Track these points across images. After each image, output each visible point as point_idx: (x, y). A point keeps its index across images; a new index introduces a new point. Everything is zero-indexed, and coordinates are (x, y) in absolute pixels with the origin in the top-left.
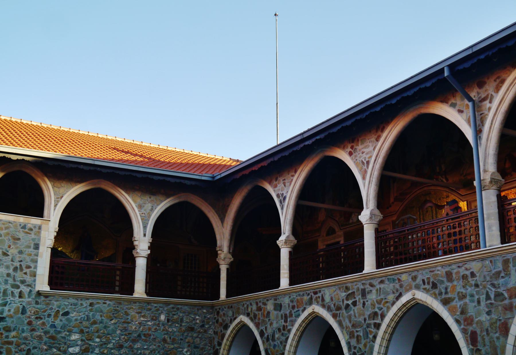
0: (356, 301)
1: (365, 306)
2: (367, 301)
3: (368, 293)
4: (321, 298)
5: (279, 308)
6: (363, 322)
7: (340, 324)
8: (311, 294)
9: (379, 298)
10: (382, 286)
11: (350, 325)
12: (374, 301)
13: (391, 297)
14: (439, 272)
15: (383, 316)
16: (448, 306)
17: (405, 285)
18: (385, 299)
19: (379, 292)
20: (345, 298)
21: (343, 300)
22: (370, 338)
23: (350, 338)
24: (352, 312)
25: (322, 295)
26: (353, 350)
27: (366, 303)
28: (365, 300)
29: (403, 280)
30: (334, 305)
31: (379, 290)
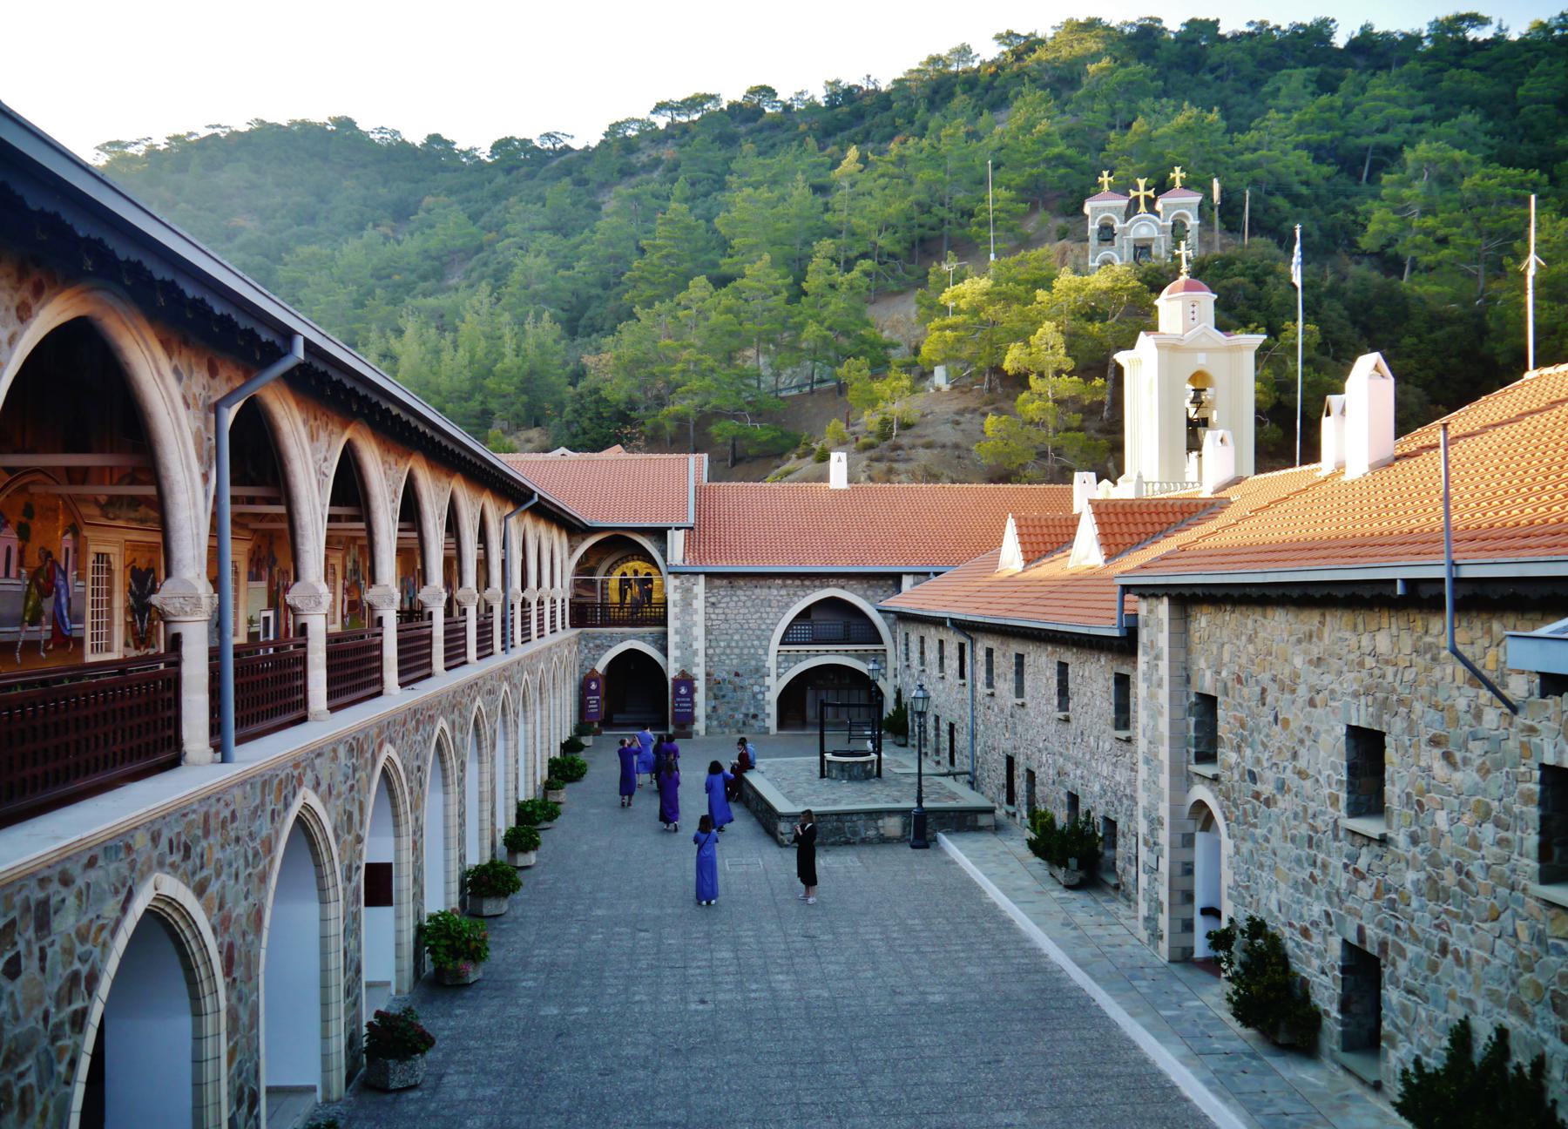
0: (18, 954)
1: (48, 964)
2: (52, 943)
3: (55, 913)
6: (40, 1026)
9: (85, 920)
10: (93, 875)
12: (69, 935)
13: (110, 908)
14: (194, 816)
15: (93, 979)
16: (203, 900)
17: (141, 859)
18: (98, 917)
19: (84, 899)
22: (59, 1073)
27: (50, 952)
28: (45, 943)
31: (85, 892)
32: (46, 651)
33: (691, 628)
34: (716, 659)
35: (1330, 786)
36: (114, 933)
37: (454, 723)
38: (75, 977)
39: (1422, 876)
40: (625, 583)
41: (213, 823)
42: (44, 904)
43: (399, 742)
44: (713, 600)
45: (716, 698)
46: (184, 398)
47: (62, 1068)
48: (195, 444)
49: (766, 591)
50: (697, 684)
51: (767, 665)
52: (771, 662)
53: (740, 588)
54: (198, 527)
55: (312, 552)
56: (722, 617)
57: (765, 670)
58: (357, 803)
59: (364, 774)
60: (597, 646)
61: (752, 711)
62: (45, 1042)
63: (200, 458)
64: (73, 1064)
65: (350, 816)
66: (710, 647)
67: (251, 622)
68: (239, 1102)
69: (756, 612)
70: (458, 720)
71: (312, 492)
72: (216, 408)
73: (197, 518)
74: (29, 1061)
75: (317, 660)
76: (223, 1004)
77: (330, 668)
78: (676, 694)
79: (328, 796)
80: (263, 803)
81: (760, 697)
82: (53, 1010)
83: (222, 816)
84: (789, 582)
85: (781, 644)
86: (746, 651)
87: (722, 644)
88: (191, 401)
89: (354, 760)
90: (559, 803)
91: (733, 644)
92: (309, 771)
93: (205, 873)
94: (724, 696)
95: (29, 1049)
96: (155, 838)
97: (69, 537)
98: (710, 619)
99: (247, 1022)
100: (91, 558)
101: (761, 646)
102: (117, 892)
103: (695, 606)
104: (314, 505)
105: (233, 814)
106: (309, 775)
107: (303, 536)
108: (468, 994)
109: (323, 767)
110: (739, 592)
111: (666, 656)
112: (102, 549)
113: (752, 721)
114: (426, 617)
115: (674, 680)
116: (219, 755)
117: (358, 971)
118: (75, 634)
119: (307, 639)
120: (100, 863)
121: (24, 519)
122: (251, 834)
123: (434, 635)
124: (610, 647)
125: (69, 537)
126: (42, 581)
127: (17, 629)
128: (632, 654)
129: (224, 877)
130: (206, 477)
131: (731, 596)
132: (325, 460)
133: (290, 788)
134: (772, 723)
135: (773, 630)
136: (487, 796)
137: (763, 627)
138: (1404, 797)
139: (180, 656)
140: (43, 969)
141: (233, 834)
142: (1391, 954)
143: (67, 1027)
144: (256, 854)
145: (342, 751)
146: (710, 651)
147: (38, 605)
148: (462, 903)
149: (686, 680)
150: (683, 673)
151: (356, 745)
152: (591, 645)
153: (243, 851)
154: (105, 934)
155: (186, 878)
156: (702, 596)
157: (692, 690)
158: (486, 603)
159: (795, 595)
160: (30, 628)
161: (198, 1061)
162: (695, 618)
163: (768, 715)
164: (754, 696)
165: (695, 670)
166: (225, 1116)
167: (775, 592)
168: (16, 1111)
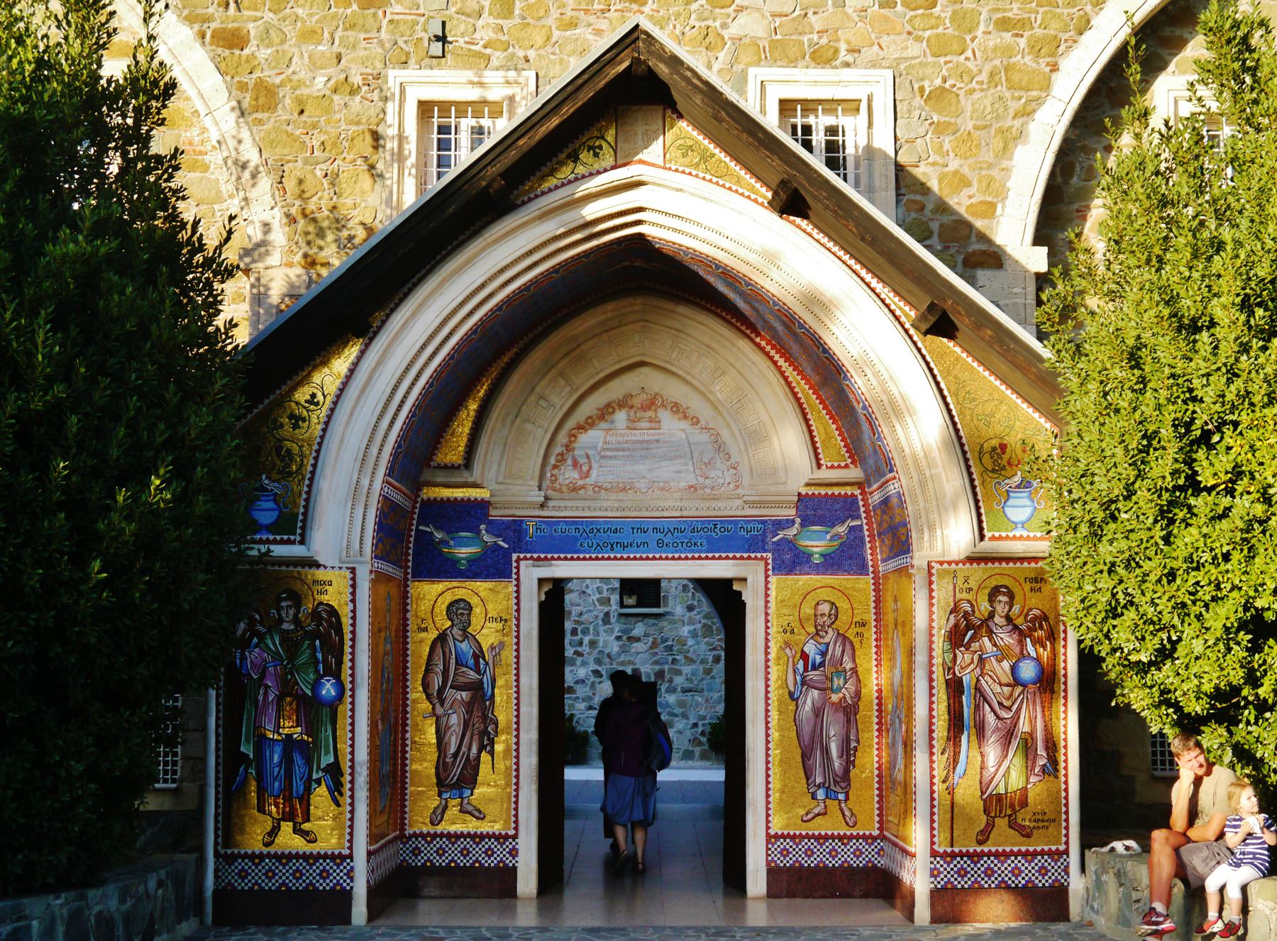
35: (600, 593)
39: (699, 626)
138: (680, 588)
142: (667, 676)
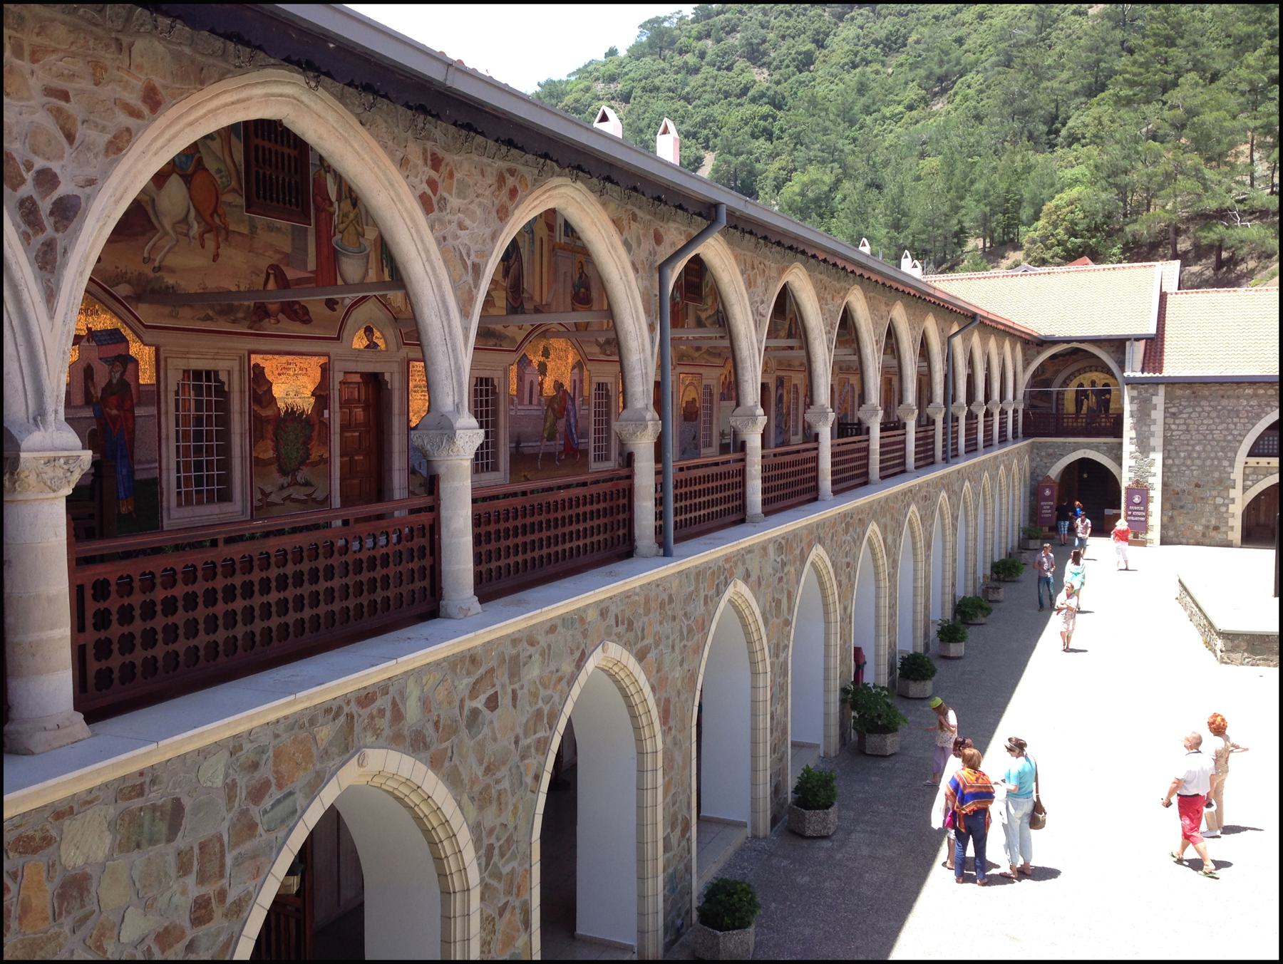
2: (522, 687)
3: (524, 665)
4: (388, 714)
5: (162, 827)
7: (453, 780)
8: (346, 710)
10: (552, 638)
11: (479, 771)
13: (567, 668)
14: (637, 598)
15: (553, 717)
18: (557, 671)
20: (467, 693)
21: (462, 701)
22: (526, 783)
23: (481, 808)
24: (486, 730)
25: (394, 704)
26: (486, 842)
27: (519, 693)
28: (516, 686)
29: (589, 619)
30: (436, 724)
32: (559, 460)
33: (1148, 438)
34: (1175, 469)
36: (571, 682)
37: (885, 526)
38: (539, 714)
40: (1081, 395)
41: (653, 605)
42: (515, 659)
43: (828, 541)
44: (1173, 410)
45: (1173, 508)
46: (633, 265)
47: (529, 780)
48: (643, 301)
49: (1233, 402)
50: (1152, 493)
51: (1232, 476)
52: (1237, 474)
53: (1205, 398)
54: (646, 368)
55: (750, 381)
56: (1184, 427)
57: (1229, 483)
58: (785, 592)
59: (792, 570)
60: (1050, 455)
61: (1213, 522)
62: (517, 758)
63: (647, 312)
64: (537, 778)
65: (778, 603)
66: (1169, 457)
67: (722, 435)
68: (673, 827)
69: (1222, 423)
70: (889, 522)
71: (751, 332)
72: (662, 269)
73: (645, 360)
74: (503, 772)
75: (754, 472)
76: (660, 746)
77: (764, 480)
78: (1130, 502)
79: (757, 587)
80: (697, 589)
81: (1223, 509)
82: (521, 736)
83: (660, 600)
84: (1261, 392)
85: (1251, 454)
86: (1208, 463)
87: (1182, 455)
88: (639, 266)
89: (783, 557)
90: (997, 601)
91: (1195, 455)
92: (740, 564)
93: (646, 642)
94: (1182, 507)
95: (504, 763)
96: (603, 614)
97: (576, 371)
98: (1170, 429)
99: (681, 764)
100: (594, 386)
101: (1226, 458)
102: (572, 653)
103: (1153, 417)
104: (752, 342)
105: (670, 597)
106: (740, 570)
107: (743, 368)
108: (884, 764)
109: (754, 565)
110: (1204, 403)
111: (1120, 465)
112: (601, 380)
113: (1213, 534)
114: (864, 431)
115: (1127, 489)
116: (661, 551)
117: (784, 732)
118: (581, 447)
119: (745, 455)
120: (560, 629)
121: (542, 359)
122: (685, 614)
123: (871, 447)
124: (1063, 456)
125: (576, 371)
126: (556, 406)
127: (538, 444)
128: (1085, 463)
129: (662, 647)
130: (651, 328)
131: (1194, 407)
132: (762, 302)
133: (722, 578)
134: (1236, 535)
135: (1241, 442)
136: (921, 592)
137: (1229, 438)
139: (632, 471)
140: (515, 706)
141: (670, 613)
143: (533, 750)
144: (690, 630)
145: (771, 550)
146: (1170, 462)
147: (554, 424)
148: (892, 683)
149: (1141, 489)
150: (1137, 482)
151: (783, 545)
152: (1043, 454)
153: (679, 627)
154: (564, 683)
155: (627, 645)
156: (1161, 407)
157: (1146, 501)
158: (928, 417)
159: (1267, 405)
160: (548, 443)
161: (641, 789)
162: (1153, 428)
163: (1232, 528)
164: (1217, 507)
165: (1151, 480)
166: (660, 835)
167: (1245, 403)
168: (495, 803)
